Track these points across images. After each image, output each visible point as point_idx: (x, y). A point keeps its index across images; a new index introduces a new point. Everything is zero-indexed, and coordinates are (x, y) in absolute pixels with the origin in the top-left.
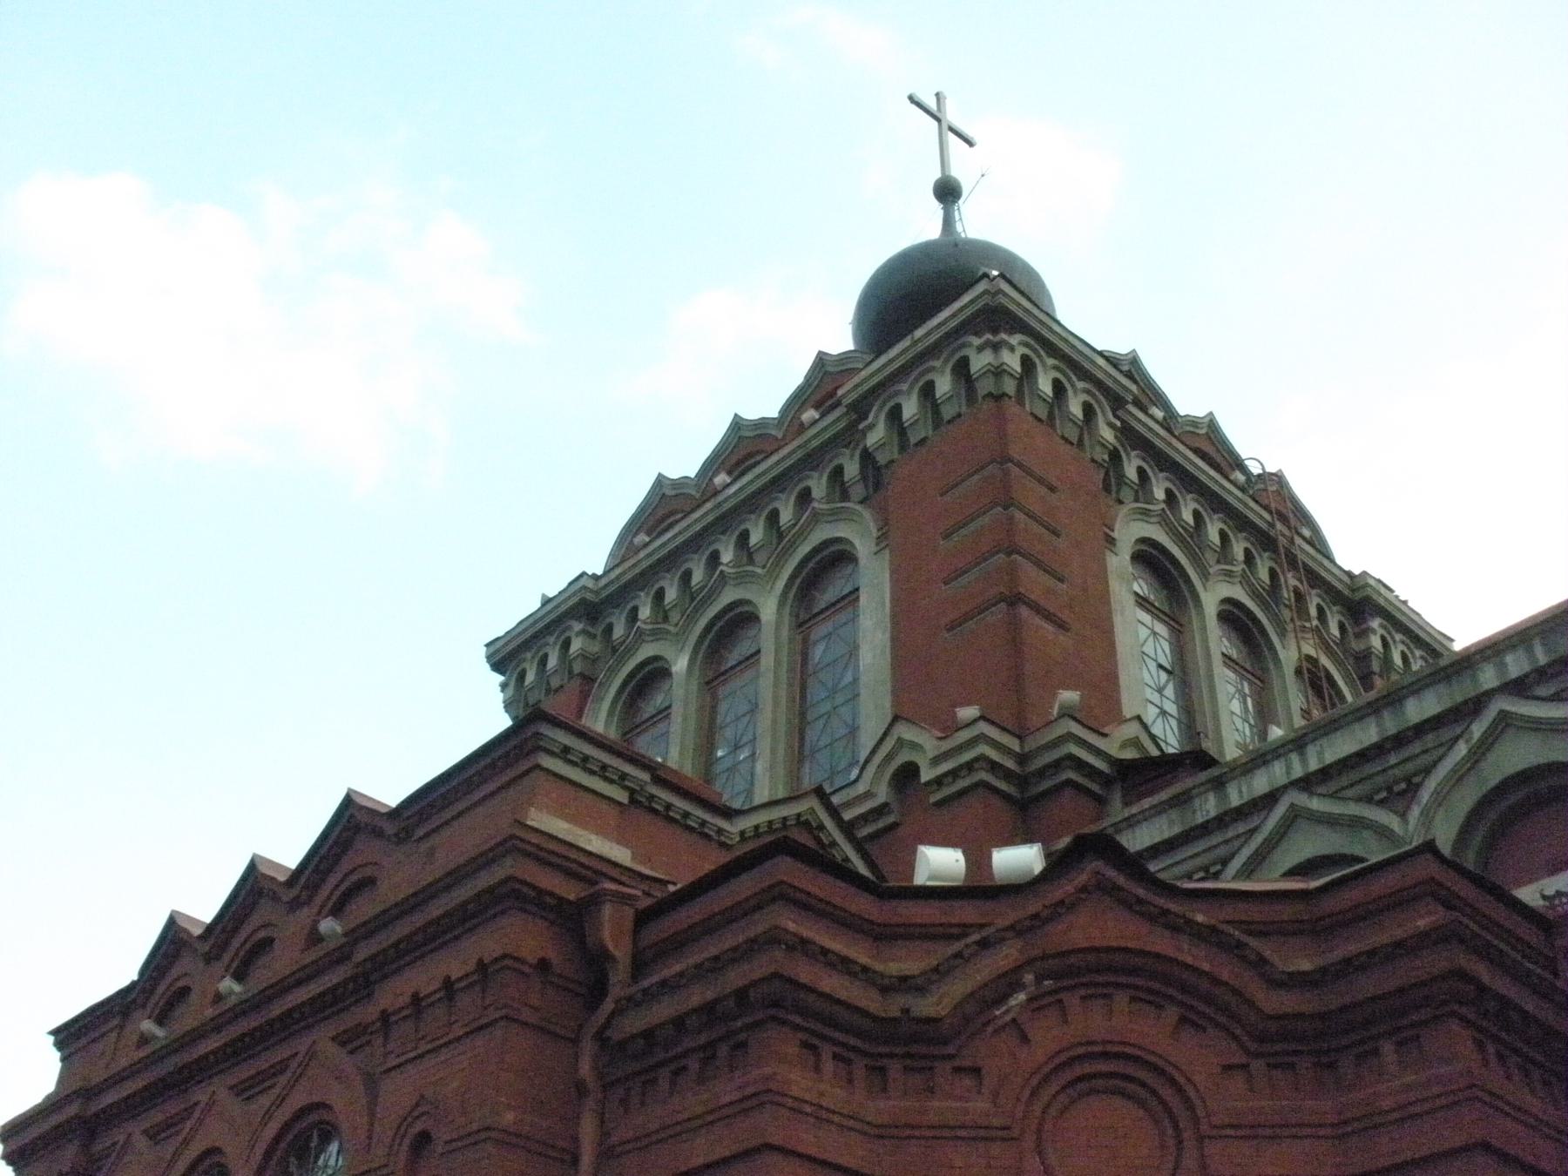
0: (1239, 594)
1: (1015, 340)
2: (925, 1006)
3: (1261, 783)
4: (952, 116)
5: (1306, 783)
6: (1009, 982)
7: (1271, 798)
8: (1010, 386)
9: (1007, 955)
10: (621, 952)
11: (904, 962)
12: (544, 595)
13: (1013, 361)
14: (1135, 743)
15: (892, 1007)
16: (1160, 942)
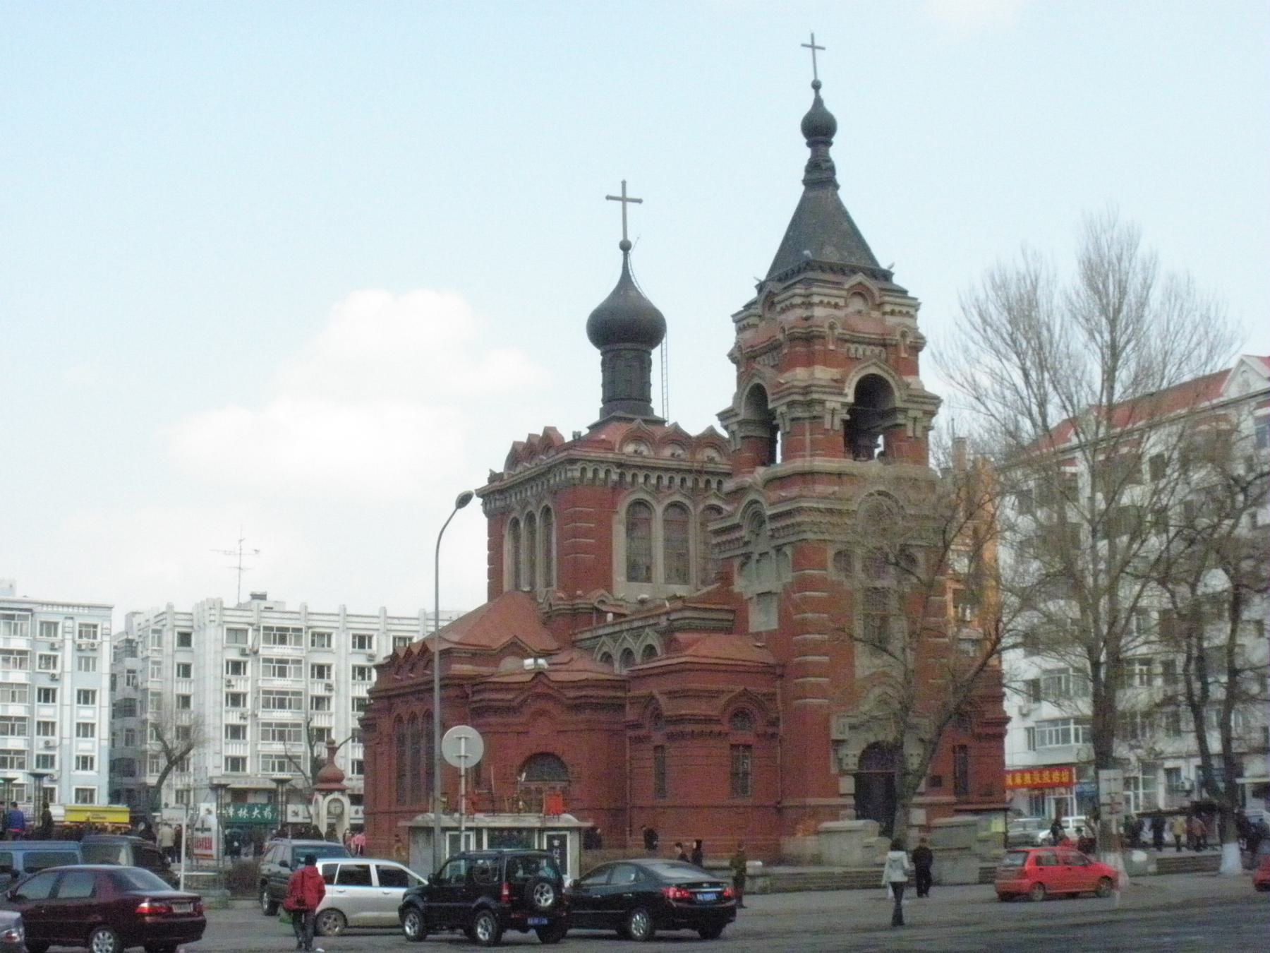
0: (677, 498)
1: (578, 464)
2: (513, 704)
3: (600, 632)
4: (629, 195)
5: (606, 635)
6: (525, 701)
7: (600, 636)
8: (577, 482)
9: (526, 694)
10: (470, 692)
11: (510, 696)
12: (491, 470)
13: (577, 474)
14: (602, 595)
15: (508, 704)
16: (551, 692)
